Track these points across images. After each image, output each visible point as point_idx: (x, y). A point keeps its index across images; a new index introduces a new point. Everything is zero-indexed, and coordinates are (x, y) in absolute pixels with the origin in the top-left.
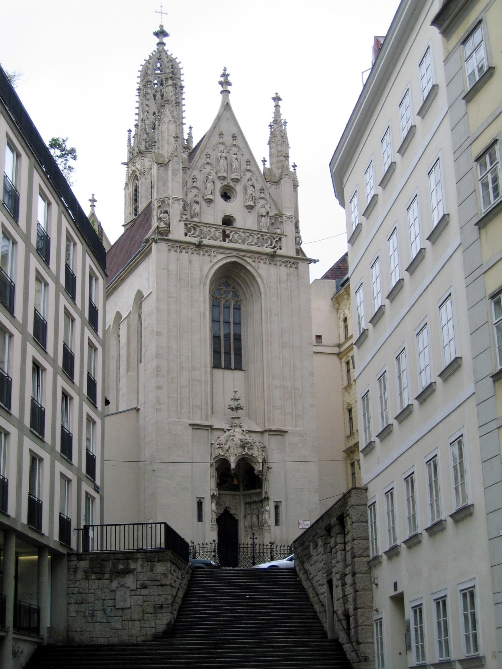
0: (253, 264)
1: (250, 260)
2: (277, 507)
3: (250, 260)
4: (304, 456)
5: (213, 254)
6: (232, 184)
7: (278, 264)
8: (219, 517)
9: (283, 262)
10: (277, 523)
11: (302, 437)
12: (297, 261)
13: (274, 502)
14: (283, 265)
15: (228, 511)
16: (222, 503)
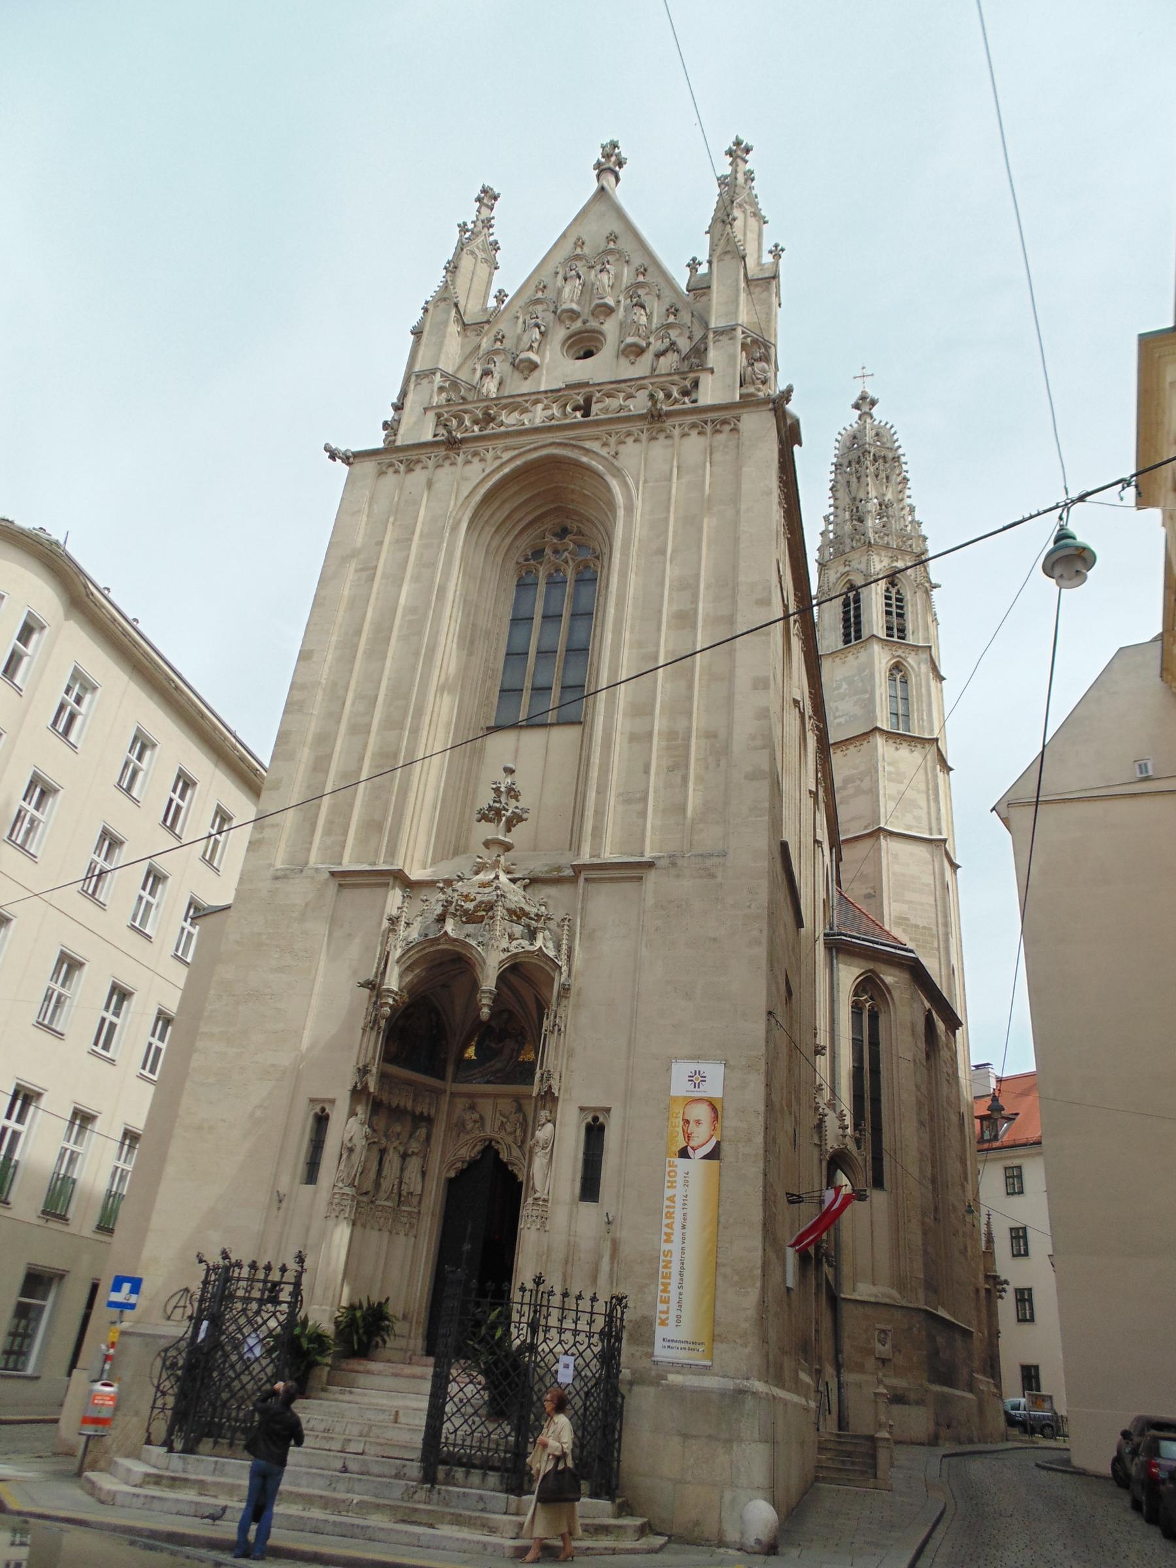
0: (603, 452)
1: (595, 446)
2: (595, 1133)
3: (595, 446)
4: (715, 940)
5: (489, 456)
6: (593, 324)
7: (676, 432)
8: (462, 1173)
9: (694, 426)
10: (590, 1188)
11: (713, 876)
12: (735, 412)
13: (582, 1109)
14: (694, 433)
15: (497, 1153)
16: (470, 1126)
